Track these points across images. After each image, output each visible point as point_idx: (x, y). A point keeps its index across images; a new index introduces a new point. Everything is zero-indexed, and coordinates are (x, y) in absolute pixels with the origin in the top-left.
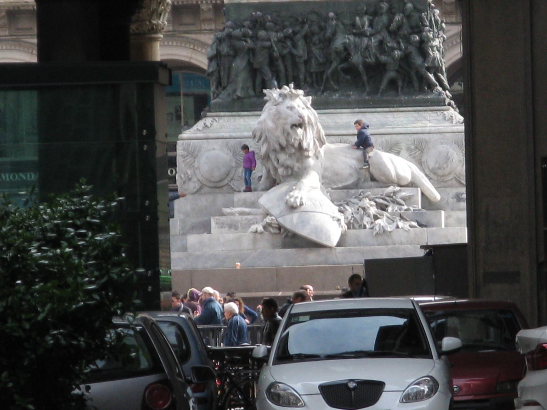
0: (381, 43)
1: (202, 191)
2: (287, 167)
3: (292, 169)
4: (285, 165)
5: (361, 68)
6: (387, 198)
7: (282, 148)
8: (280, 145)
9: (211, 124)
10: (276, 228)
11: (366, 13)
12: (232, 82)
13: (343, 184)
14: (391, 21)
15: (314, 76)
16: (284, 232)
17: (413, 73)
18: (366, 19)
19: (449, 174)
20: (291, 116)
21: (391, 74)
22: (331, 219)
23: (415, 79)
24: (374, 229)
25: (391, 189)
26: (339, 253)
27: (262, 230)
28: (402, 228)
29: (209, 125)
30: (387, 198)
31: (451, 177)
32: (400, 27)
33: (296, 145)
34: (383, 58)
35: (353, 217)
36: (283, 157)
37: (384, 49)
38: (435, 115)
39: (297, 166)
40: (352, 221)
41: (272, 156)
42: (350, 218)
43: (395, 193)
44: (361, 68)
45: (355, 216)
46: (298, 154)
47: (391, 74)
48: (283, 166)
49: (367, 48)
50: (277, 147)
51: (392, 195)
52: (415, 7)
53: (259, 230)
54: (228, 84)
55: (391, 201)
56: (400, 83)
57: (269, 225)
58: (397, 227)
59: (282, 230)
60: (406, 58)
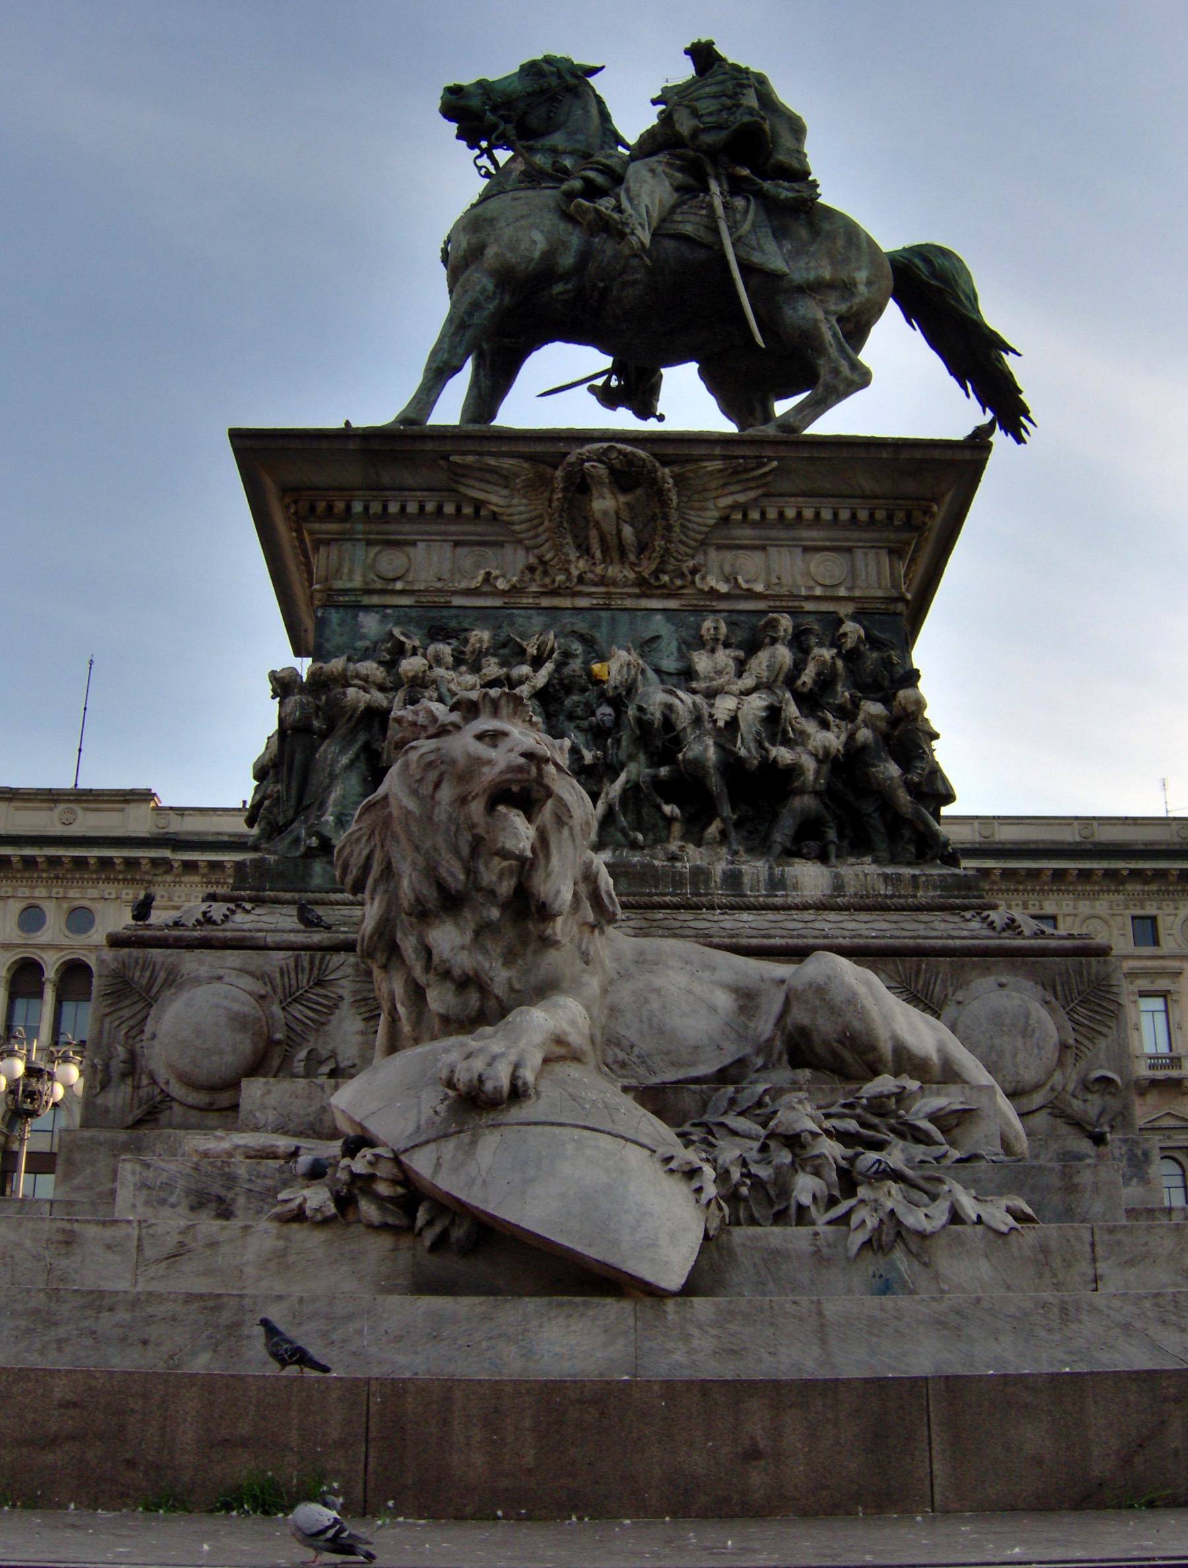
0: (773, 714)
1: (164, 1117)
2: (466, 982)
3: (484, 990)
4: (457, 972)
5: (715, 782)
7: (451, 902)
8: (441, 886)
9: (226, 916)
10: (390, 1199)
12: (308, 807)
14: (799, 667)
16: (430, 1223)
17: (869, 807)
19: (1038, 1086)
20: (490, 762)
21: (804, 803)
22: (659, 1170)
23: (876, 821)
24: (855, 1220)
27: (332, 1209)
28: (979, 1220)
29: (218, 917)
32: (825, 681)
33: (506, 888)
34: (783, 755)
35: (748, 1175)
36: (448, 939)
37: (785, 732)
38: (957, 919)
39: (501, 977)
40: (744, 1191)
41: (408, 945)
42: (736, 1175)
44: (715, 782)
45: (754, 1169)
46: (510, 933)
47: (804, 803)
48: (446, 974)
49: (733, 723)
50: (430, 894)
52: (869, 638)
53: (311, 1204)
54: (297, 813)
56: (832, 835)
57: (363, 1183)
58: (956, 1217)
59: (422, 1216)
60: (848, 766)
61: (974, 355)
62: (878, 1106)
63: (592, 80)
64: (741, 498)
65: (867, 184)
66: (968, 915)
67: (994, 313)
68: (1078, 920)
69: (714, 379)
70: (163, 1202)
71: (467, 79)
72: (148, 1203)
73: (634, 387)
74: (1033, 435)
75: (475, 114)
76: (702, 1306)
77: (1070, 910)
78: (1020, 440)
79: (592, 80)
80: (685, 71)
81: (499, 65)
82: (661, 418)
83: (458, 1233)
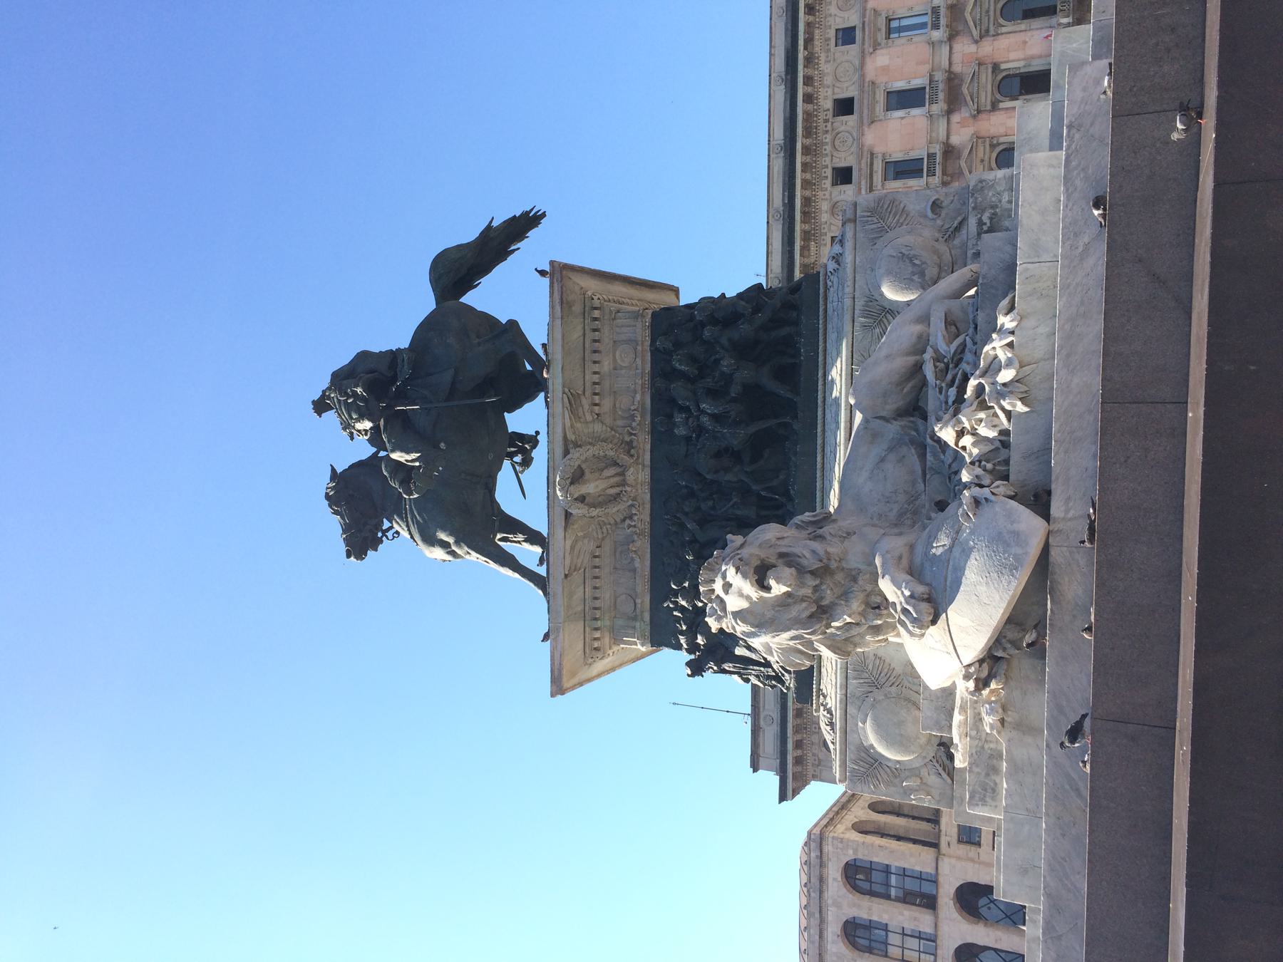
6: (949, 377)
11: (670, 416)
13: (920, 480)
14: (683, 375)
15: (764, 513)
16: (1004, 649)
18: (679, 418)
25: (929, 371)
26: (1067, 511)
30: (949, 377)
31: (942, 248)
32: (693, 360)
34: (735, 390)
35: (980, 461)
40: (989, 466)
43: (938, 358)
51: (941, 365)
55: (956, 366)
59: (999, 654)
61: (497, 244)
62: (941, 374)
63: (339, 471)
64: (586, 407)
65: (394, 316)
66: (829, 283)
67: (470, 234)
68: (835, 154)
69: (514, 405)
70: (994, 790)
71: (343, 548)
72: (993, 799)
73: (523, 445)
74: (541, 207)
75: (361, 540)
76: (1056, 509)
77: (828, 159)
78: (544, 215)
79: (339, 471)
80: (331, 416)
81: (331, 526)
82: (537, 433)
83: (1010, 635)
